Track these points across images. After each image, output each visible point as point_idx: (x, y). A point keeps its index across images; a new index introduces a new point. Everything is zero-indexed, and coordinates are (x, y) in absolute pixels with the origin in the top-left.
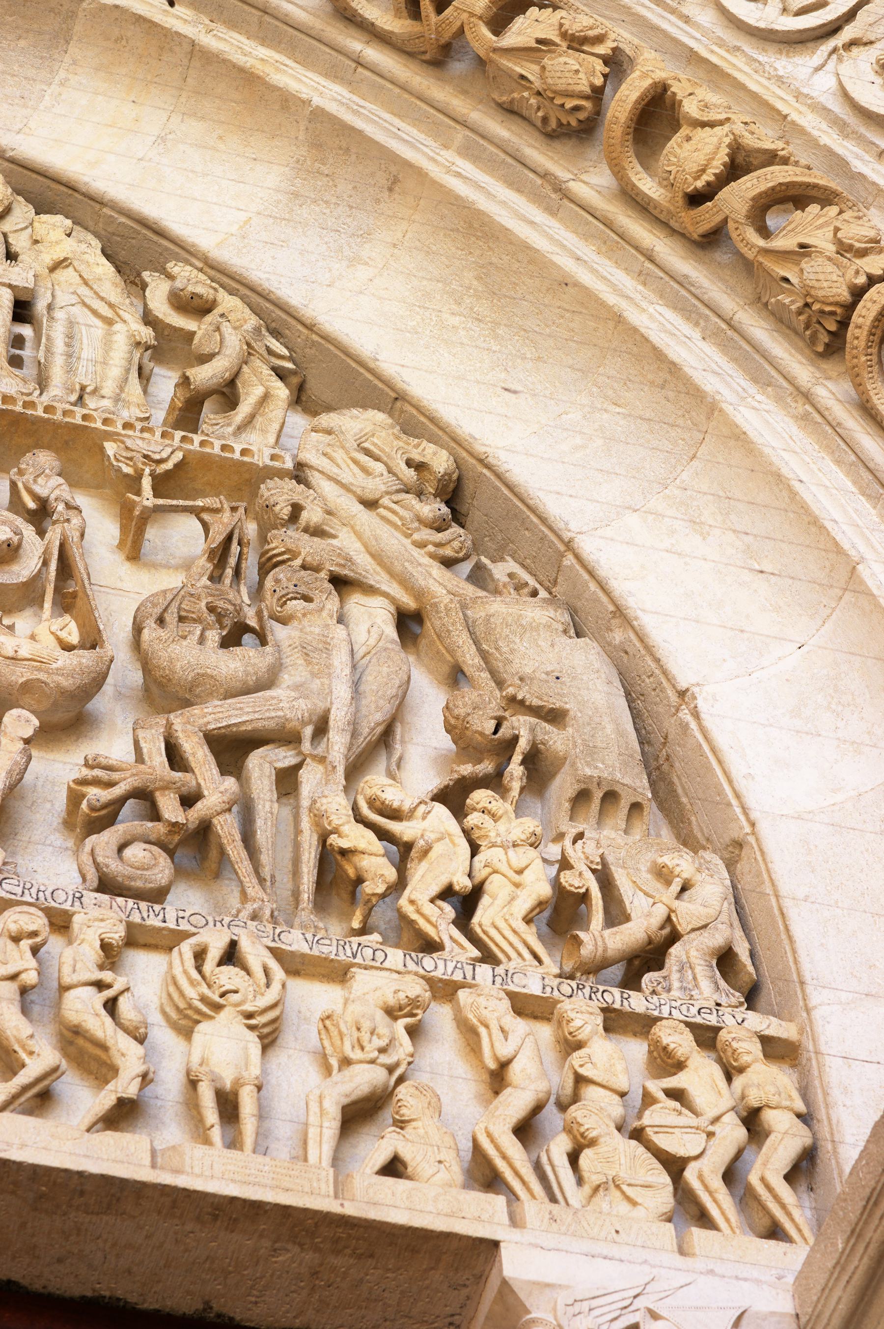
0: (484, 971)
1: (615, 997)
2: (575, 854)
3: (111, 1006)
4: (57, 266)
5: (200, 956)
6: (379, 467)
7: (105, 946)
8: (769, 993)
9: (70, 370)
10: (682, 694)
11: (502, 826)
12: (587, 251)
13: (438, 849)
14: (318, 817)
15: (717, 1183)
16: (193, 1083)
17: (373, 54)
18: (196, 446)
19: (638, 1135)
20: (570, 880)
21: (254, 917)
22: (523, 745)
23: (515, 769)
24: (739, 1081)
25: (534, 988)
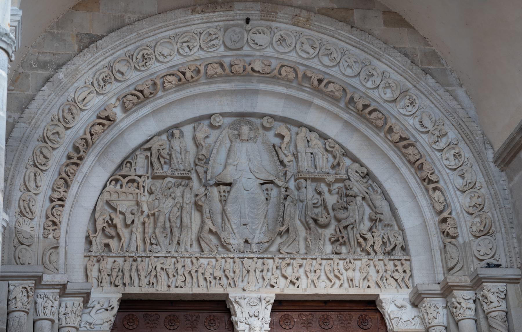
0: (376, 257)
1: (390, 257)
2: (384, 237)
3: (339, 272)
4: (315, 145)
5: (347, 262)
6: (358, 175)
7: (338, 263)
8: (407, 250)
9: (319, 165)
10: (396, 209)
11: (376, 233)
12: (382, 142)
13: (370, 239)
14: (356, 237)
15: (401, 282)
16: (348, 280)
17: (352, 113)
18: (337, 177)
19: (393, 277)
20: (384, 240)
21: (352, 254)
22: (378, 220)
23: (377, 223)
24: (403, 266)
25: (381, 258)
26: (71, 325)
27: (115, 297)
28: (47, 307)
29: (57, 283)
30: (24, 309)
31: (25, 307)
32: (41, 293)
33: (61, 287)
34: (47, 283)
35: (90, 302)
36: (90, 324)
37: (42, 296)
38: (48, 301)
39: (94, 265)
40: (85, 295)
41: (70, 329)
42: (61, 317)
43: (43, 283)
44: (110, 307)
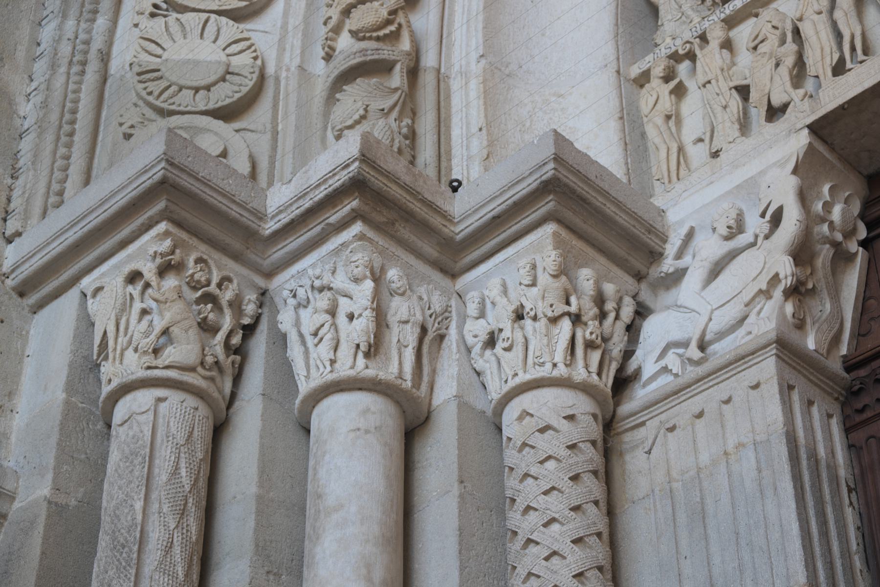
26: (523, 377)
27: (781, 164)
28: (321, 333)
29: (320, 194)
30: (142, 374)
31: (146, 358)
32: (292, 284)
33: (355, 203)
34: (285, 218)
35: (671, 249)
36: (685, 344)
37: (301, 293)
38: (322, 301)
39: (679, 91)
40: (548, 205)
41: (525, 401)
42: (479, 364)
43: (270, 227)
44: (763, 215)
